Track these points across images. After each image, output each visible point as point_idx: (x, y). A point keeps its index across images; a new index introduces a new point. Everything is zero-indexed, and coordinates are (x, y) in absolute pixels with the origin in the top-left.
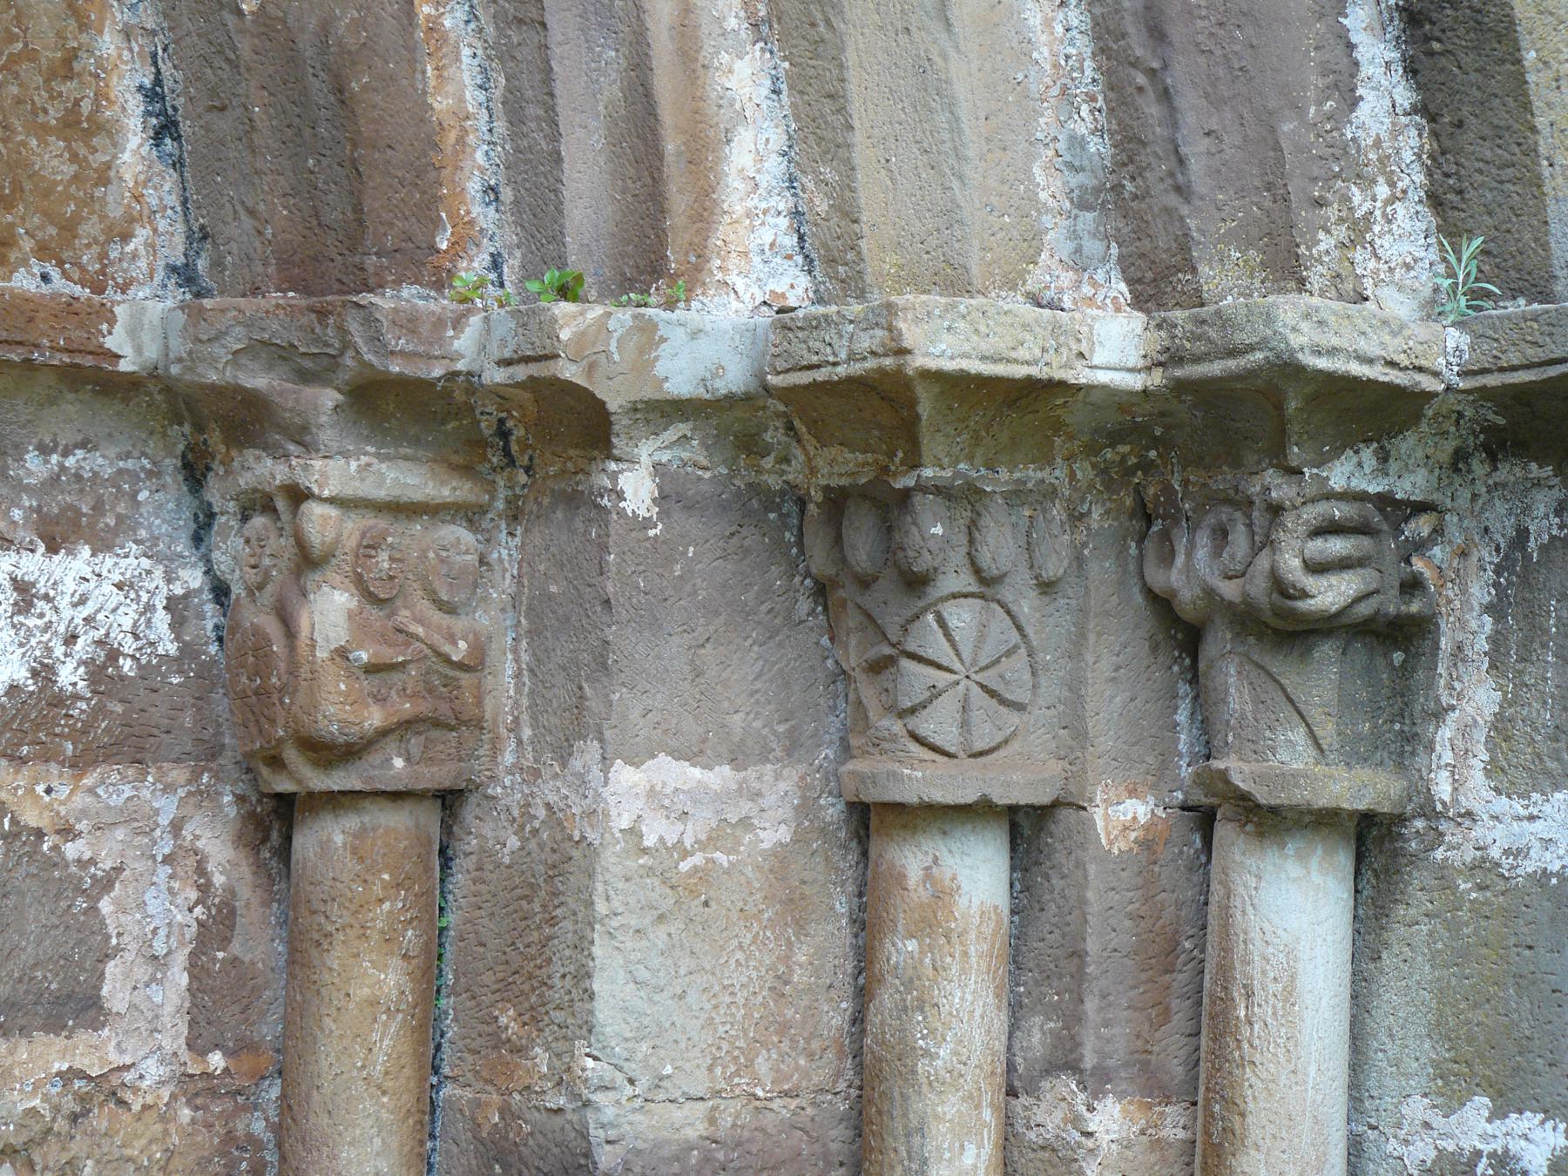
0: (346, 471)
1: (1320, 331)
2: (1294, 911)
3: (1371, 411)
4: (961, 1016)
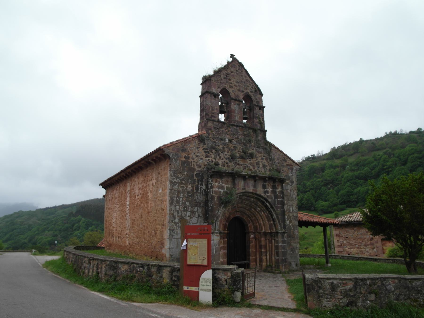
0: (257, 234)
1: (273, 231)
2: (273, 241)
4: (268, 243)
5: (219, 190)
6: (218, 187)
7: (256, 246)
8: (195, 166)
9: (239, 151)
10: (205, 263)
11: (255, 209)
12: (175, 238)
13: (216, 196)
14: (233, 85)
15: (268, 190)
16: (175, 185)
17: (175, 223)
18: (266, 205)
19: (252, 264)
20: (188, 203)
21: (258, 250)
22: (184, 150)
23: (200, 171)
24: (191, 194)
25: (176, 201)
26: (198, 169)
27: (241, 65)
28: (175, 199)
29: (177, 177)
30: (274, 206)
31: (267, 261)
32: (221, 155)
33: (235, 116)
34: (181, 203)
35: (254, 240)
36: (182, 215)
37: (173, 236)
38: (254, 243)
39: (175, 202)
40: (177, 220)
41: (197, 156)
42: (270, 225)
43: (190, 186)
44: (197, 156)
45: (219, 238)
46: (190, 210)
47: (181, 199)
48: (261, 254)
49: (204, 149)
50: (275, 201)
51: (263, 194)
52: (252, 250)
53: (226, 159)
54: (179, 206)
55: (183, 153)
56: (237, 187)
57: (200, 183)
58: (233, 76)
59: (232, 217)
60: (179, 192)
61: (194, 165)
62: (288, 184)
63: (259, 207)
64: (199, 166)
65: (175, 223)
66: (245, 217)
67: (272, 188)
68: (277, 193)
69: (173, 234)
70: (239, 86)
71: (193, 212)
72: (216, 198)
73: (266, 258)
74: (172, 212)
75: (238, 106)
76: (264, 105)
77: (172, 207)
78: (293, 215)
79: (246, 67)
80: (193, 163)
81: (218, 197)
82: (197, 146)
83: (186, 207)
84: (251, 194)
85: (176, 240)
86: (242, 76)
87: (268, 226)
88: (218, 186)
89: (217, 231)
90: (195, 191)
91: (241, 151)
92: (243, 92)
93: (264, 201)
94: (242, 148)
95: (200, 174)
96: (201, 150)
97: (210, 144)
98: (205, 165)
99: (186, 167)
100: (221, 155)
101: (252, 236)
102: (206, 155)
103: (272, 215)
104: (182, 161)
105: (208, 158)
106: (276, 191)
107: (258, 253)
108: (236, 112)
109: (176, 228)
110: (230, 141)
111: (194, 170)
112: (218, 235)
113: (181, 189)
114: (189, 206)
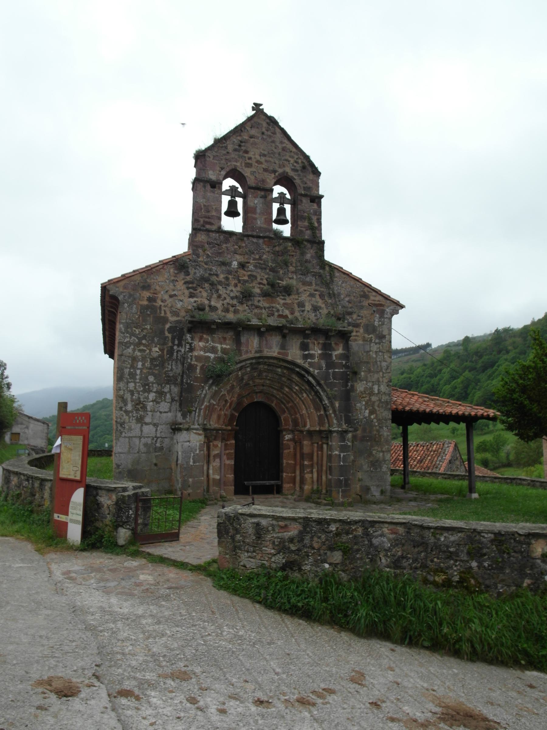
0: (296, 433)
2: (325, 446)
3: (325, 431)
4: (315, 449)
5: (207, 354)
6: (205, 349)
7: (295, 455)
8: (168, 313)
9: (260, 283)
10: (78, 478)
11: (291, 389)
12: (125, 437)
13: (199, 365)
14: (253, 162)
15: (312, 352)
16: (128, 347)
17: (127, 412)
18: (308, 380)
19: (286, 486)
20: (151, 379)
21: (298, 461)
22: (146, 287)
23: (177, 322)
24: (159, 363)
25: (129, 375)
26: (173, 319)
27: (272, 122)
28: (127, 371)
29: (133, 334)
30: (322, 382)
31: (313, 482)
32: (220, 292)
33: (255, 219)
34: (138, 377)
35: (292, 445)
36: (139, 398)
37: (121, 433)
38: (292, 450)
39: (127, 376)
40: (129, 407)
41: (171, 296)
42: (320, 417)
43: (157, 349)
44: (171, 296)
45: (202, 438)
46: (155, 390)
47: (138, 372)
48: (302, 467)
49: (185, 283)
50: (328, 374)
51: (300, 361)
52: (287, 461)
53: (232, 298)
54: (135, 383)
55: (145, 292)
56: (244, 348)
57: (176, 342)
58: (255, 144)
59: (246, 402)
60: (134, 359)
61: (165, 311)
62: (371, 340)
63: (297, 385)
64: (175, 313)
65: (127, 412)
66: (275, 402)
67: (322, 349)
68: (334, 358)
69: (122, 430)
70: (266, 161)
71: (161, 394)
72: (198, 368)
73: (312, 478)
74: (121, 393)
75: (262, 200)
76: (321, 192)
77: (122, 385)
78: (380, 400)
79: (282, 124)
80: (163, 308)
81: (202, 368)
82: (172, 278)
83: (148, 385)
84: (275, 361)
85: (127, 439)
86: (273, 142)
87: (317, 419)
88: (205, 347)
89: (196, 426)
90: (166, 357)
91: (265, 282)
92: (274, 172)
93: (303, 372)
94: (266, 276)
95: (176, 327)
96: (180, 285)
97: (200, 272)
98: (187, 311)
99: (149, 315)
100: (222, 291)
101: (288, 437)
102: (191, 293)
103: (321, 400)
104: (141, 306)
105: (195, 299)
106: (331, 355)
107: (298, 467)
108: (258, 211)
109: (127, 420)
110: (242, 266)
111: (165, 320)
112: (201, 432)
113: (139, 354)
114: (153, 383)
